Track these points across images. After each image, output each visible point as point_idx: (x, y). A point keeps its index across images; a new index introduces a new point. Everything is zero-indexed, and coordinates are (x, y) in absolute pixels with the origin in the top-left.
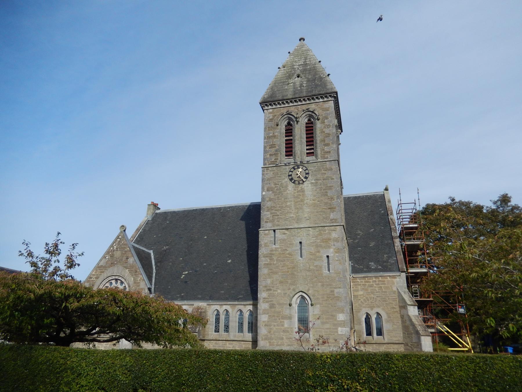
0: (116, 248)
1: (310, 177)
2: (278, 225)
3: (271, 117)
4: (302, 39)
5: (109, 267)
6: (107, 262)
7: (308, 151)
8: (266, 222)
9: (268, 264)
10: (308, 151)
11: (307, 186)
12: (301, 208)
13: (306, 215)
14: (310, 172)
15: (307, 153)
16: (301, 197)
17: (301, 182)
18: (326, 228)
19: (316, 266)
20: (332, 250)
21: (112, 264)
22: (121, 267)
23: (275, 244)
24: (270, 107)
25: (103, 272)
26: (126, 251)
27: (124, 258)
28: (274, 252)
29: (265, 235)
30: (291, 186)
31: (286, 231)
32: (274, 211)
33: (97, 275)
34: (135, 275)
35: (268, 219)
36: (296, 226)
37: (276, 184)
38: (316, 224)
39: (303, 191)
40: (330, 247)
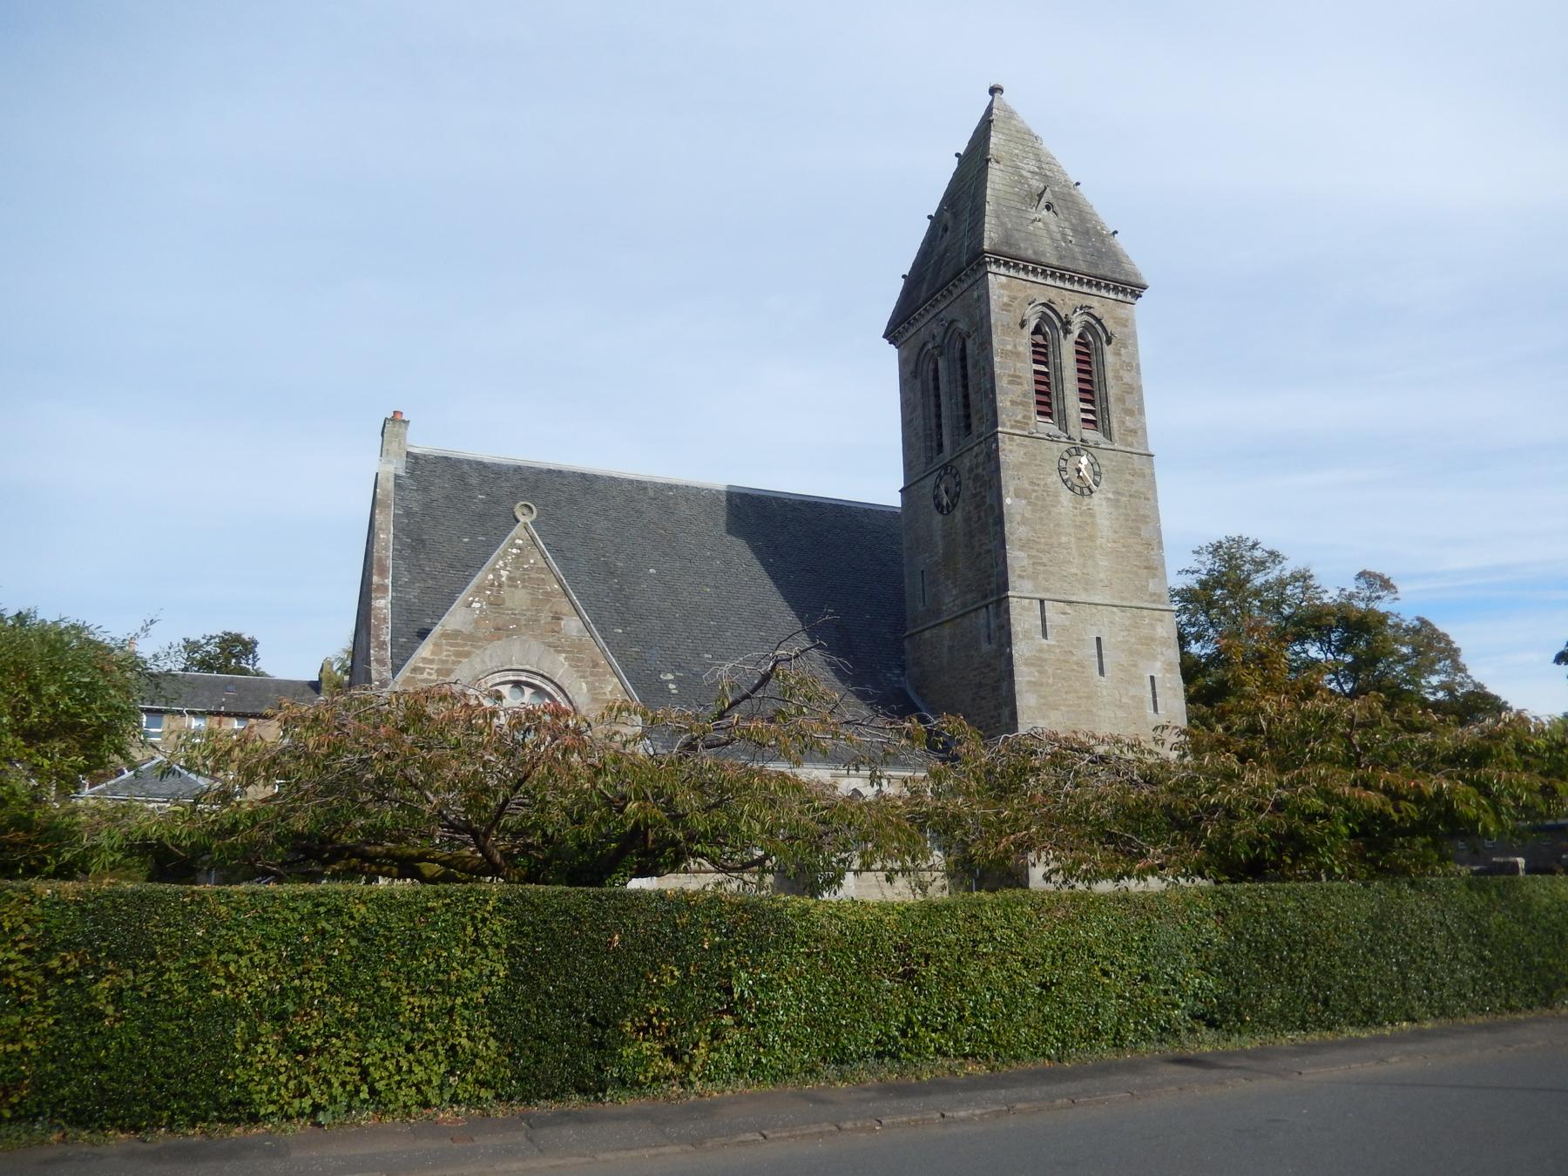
0: (509, 578)
1: (1103, 485)
2: (1047, 590)
3: (1006, 299)
4: (994, 90)
5: (490, 641)
6: (476, 622)
7: (1083, 416)
8: (1021, 577)
9: (1035, 684)
10: (1083, 416)
11: (1099, 502)
12: (1092, 557)
13: (1102, 576)
14: (1103, 470)
15: (1084, 420)
16: (1088, 528)
17: (1086, 491)
18: (1145, 612)
19: (1133, 697)
20: (1158, 664)
21: (500, 631)
22: (536, 647)
23: (1045, 635)
24: (1002, 270)
25: (467, 655)
26: (546, 594)
27: (545, 617)
28: (1046, 656)
29: (1023, 608)
30: (1066, 496)
31: (1068, 609)
32: (1034, 553)
33: (443, 662)
34: (592, 674)
35: (1023, 569)
36: (1082, 597)
37: (1032, 483)
38: (1123, 599)
39: (1090, 513)
40: (1154, 658)
